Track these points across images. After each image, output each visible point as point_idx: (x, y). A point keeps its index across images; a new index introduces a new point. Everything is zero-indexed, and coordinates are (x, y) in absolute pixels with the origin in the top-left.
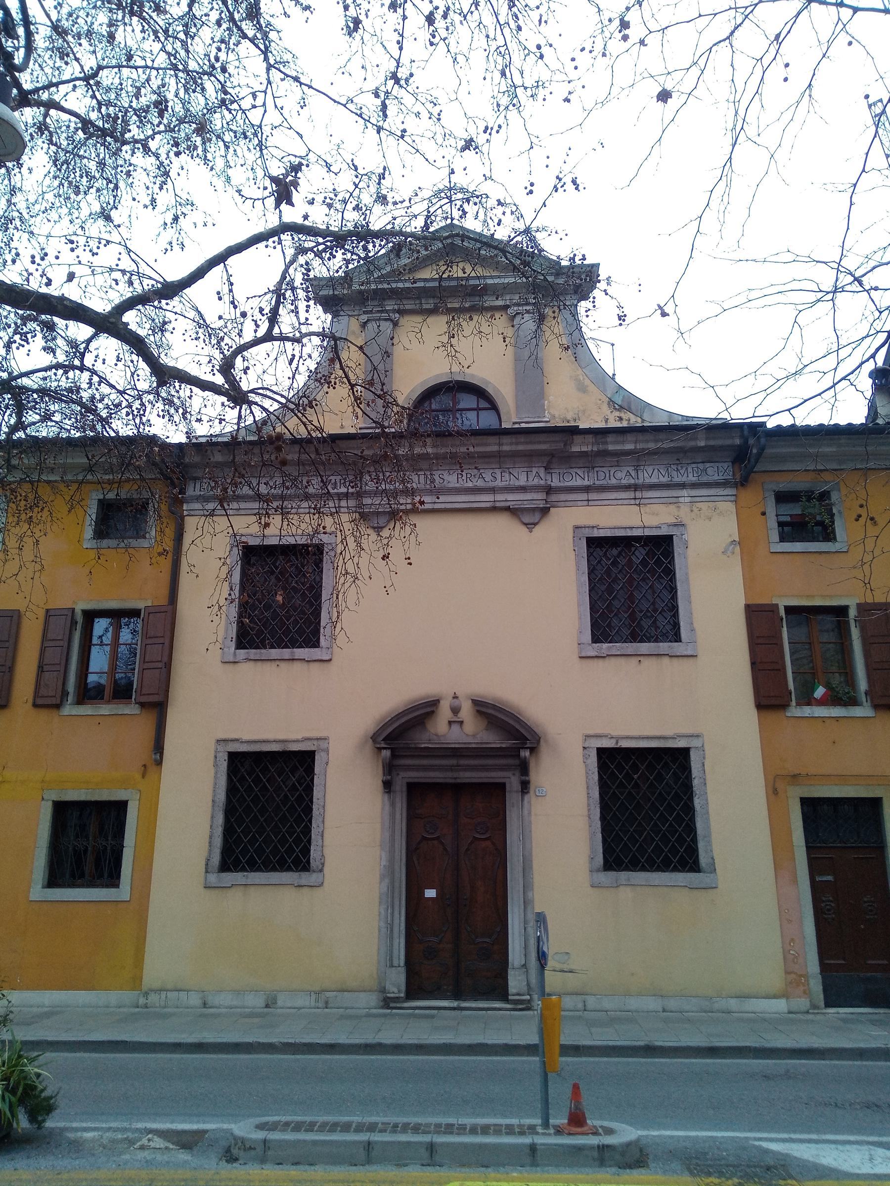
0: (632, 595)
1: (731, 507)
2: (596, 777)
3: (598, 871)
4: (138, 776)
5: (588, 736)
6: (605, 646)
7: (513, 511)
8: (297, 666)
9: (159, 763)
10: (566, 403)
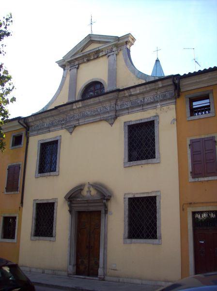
0: (141, 144)
1: (173, 106)
2: (127, 208)
3: (126, 238)
4: (18, 210)
5: (125, 194)
6: (132, 162)
7: (106, 120)
8: (51, 177)
9: (22, 206)
10: (125, 80)
